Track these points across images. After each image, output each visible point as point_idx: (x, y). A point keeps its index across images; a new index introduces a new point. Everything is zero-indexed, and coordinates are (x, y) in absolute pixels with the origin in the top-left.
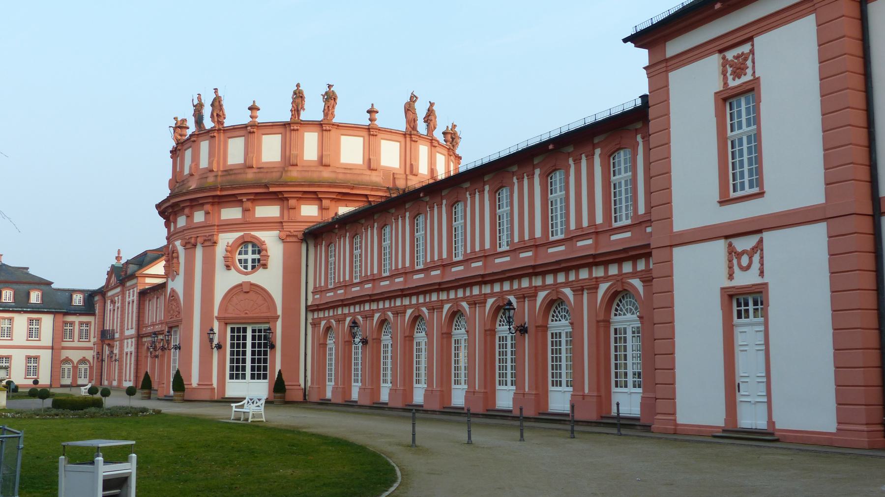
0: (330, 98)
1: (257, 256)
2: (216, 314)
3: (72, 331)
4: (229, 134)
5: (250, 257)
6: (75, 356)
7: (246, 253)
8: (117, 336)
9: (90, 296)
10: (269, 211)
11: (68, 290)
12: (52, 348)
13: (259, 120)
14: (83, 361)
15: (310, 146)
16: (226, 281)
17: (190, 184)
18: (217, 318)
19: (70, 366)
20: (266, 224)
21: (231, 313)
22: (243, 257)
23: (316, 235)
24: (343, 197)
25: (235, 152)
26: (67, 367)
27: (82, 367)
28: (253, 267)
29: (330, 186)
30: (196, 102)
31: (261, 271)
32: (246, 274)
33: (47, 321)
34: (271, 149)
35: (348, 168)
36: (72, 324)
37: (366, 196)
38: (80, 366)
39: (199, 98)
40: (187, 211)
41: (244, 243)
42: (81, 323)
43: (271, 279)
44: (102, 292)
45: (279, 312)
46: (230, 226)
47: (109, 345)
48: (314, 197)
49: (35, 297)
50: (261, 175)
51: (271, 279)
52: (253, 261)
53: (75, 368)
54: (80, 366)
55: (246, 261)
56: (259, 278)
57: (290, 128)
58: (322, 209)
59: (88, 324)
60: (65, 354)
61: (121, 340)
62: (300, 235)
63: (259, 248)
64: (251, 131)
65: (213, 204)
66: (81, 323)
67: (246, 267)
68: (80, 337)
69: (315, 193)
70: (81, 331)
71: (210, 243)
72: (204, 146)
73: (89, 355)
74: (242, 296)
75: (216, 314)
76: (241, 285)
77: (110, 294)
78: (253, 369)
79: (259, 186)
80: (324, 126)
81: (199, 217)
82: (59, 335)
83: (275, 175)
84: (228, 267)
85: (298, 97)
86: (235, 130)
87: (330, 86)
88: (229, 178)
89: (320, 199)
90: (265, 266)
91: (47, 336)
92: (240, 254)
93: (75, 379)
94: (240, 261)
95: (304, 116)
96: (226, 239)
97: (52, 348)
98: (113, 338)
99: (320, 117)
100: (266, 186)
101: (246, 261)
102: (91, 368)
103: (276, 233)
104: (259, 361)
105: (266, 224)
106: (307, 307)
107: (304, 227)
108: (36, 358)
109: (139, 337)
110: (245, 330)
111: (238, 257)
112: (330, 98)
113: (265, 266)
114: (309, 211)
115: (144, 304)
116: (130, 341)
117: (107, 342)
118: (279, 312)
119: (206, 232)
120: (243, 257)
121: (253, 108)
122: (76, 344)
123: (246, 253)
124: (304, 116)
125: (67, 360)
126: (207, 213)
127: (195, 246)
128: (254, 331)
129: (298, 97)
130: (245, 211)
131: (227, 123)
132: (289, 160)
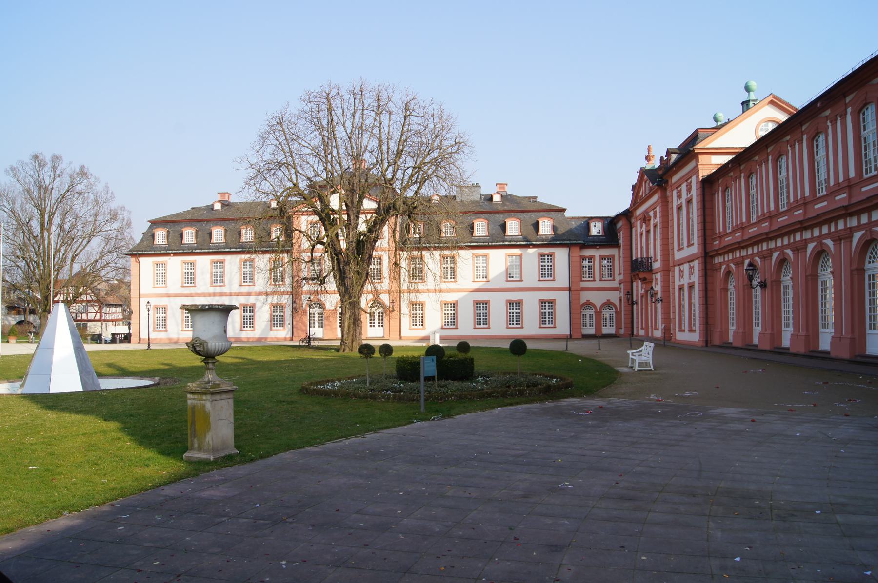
3: (591, 269)
6: (598, 299)
8: (657, 265)
9: (610, 223)
14: (608, 304)
19: (592, 312)
26: (588, 312)
27: (607, 313)
33: (561, 256)
36: (591, 259)
44: (627, 215)
47: (644, 280)
49: (546, 228)
53: (598, 314)
59: (610, 258)
60: (585, 297)
61: (667, 270)
66: (602, 258)
68: (601, 276)
70: (602, 266)
73: (614, 297)
77: (639, 212)
82: (575, 273)
91: (562, 277)
93: (598, 328)
97: (570, 289)
98: (649, 270)
102: (618, 313)
108: (551, 303)
109: (707, 256)
115: (712, 201)
116: (686, 267)
117: (642, 276)
122: (598, 284)
125: (588, 304)
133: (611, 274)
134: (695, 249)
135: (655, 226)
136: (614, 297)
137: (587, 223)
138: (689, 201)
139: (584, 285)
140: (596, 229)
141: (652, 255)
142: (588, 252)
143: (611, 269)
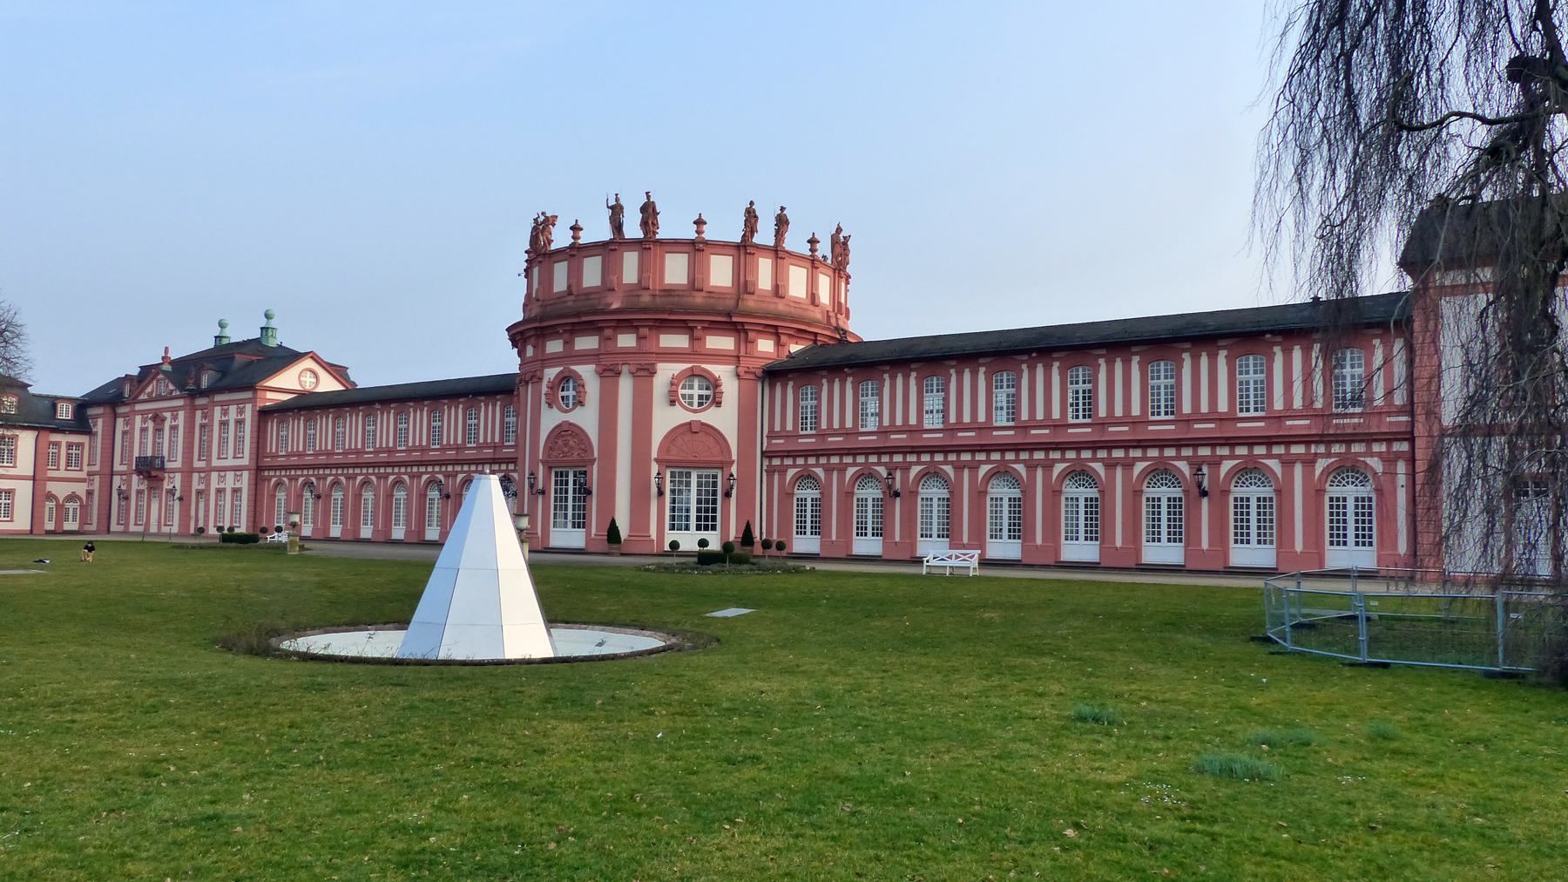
0: (782, 222)
1: (705, 392)
2: (654, 455)
4: (667, 248)
5: (696, 392)
6: (60, 490)
7: (691, 387)
10: (722, 342)
11: (47, 397)
12: (34, 479)
13: (707, 236)
14: (72, 497)
15: (764, 271)
16: (665, 419)
17: (609, 300)
18: (657, 460)
20: (718, 357)
21: (674, 455)
22: (687, 392)
23: (774, 374)
24: (799, 334)
25: (675, 270)
27: (71, 506)
28: (700, 404)
29: (792, 321)
30: (612, 202)
31: (713, 408)
32: (695, 411)
34: (720, 272)
35: (797, 302)
36: (57, 444)
37: (816, 334)
38: (68, 505)
39: (617, 200)
40: (608, 332)
41: (692, 374)
42: (70, 446)
43: (724, 419)
45: (734, 457)
46: (672, 355)
48: (775, 332)
50: (712, 301)
51: (724, 419)
52: (700, 397)
53: (60, 507)
54: (68, 505)
55: (691, 397)
56: (710, 417)
57: (744, 249)
58: (778, 344)
62: (759, 372)
63: (714, 384)
64: (697, 248)
65: (651, 328)
66: (70, 446)
67: (691, 404)
68: (68, 464)
69: (776, 327)
70: (69, 456)
71: (645, 373)
72: (630, 261)
73: (81, 489)
74: (688, 436)
75: (654, 455)
76: (690, 424)
78: (699, 518)
79: (719, 313)
80: (777, 252)
81: (626, 341)
83: (730, 303)
84: (672, 403)
85: (751, 217)
86: (675, 245)
87: (782, 209)
88: (670, 299)
89: (692, 329)
90: (719, 404)
92: (684, 387)
93: (59, 522)
94: (684, 396)
95: (757, 239)
96: (666, 371)
97: (34, 479)
99: (771, 242)
100: (729, 315)
101: (691, 397)
103: (732, 367)
104: (707, 510)
105: (718, 357)
106: (763, 453)
107: (763, 363)
110: (688, 475)
111: (681, 392)
112: (782, 222)
113: (719, 404)
114: (766, 346)
118: (734, 457)
119: (644, 360)
120: (687, 392)
121: (699, 222)
122: (62, 473)
123: (691, 387)
124: (757, 239)
125: (50, 496)
126: (639, 338)
127: (619, 374)
128: (699, 477)
129: (751, 217)
130: (693, 339)
131: (662, 234)
132: (744, 285)
133: (79, 463)
134: (245, 461)
135: (174, 428)
136: (81, 489)
137: (54, 401)
138: (240, 422)
139: (51, 474)
140: (65, 413)
141: (165, 453)
142: (55, 437)
143: (79, 458)
